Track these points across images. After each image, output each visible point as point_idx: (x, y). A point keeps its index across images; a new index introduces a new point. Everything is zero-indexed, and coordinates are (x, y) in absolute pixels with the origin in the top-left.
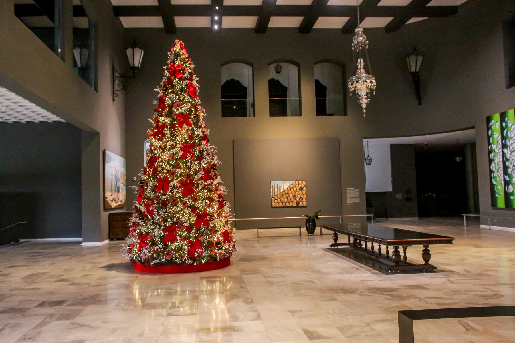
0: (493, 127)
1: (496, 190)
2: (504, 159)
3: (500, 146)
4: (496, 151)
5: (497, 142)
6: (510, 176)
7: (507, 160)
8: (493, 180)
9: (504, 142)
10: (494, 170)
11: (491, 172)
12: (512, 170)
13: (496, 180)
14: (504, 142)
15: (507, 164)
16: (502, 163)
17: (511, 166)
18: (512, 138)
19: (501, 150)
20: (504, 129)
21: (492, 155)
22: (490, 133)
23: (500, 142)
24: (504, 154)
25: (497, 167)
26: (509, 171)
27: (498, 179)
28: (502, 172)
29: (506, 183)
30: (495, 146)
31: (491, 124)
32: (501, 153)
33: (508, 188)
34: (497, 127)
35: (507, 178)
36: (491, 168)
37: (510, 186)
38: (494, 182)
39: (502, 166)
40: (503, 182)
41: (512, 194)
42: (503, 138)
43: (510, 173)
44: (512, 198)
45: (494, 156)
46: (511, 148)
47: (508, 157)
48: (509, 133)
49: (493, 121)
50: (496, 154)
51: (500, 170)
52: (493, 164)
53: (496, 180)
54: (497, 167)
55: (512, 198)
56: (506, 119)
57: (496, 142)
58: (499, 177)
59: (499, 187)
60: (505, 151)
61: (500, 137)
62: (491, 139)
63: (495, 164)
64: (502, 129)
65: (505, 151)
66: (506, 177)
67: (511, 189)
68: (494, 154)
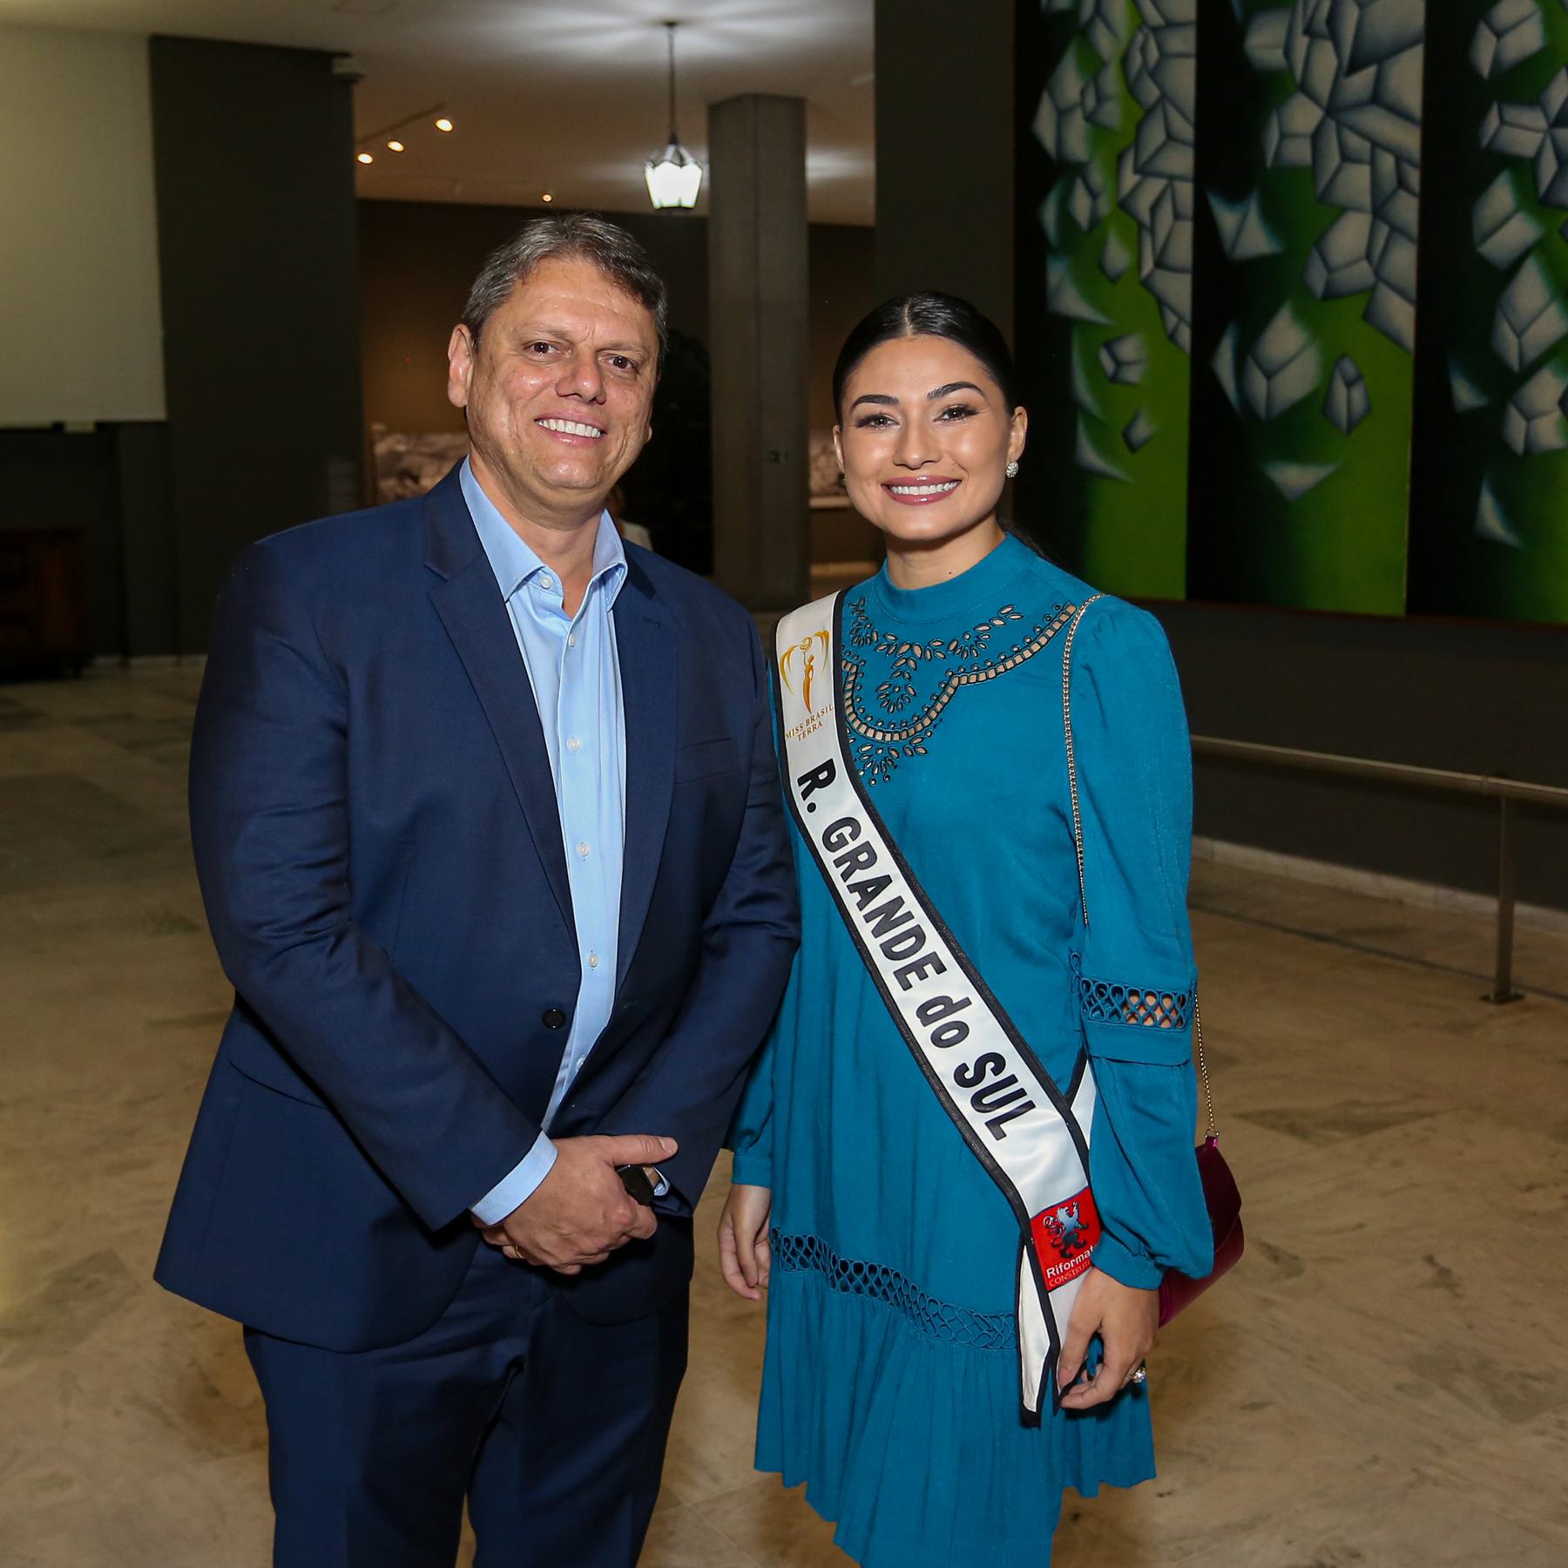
6: (1299, 207)
8: (1057, 272)
12: (1334, 109)
15: (1265, 42)
16: (1184, 41)
17: (1326, 62)
28: (1182, 161)
29: (1232, 297)
33: (1245, 352)
37: (1285, 337)
41: (1300, 429)
43: (1299, 152)
44: (1293, 477)
53: (1095, 275)
55: (1293, 477)
58: (1141, 230)
59: (1129, 349)
63: (1094, 68)
66: (1227, 218)
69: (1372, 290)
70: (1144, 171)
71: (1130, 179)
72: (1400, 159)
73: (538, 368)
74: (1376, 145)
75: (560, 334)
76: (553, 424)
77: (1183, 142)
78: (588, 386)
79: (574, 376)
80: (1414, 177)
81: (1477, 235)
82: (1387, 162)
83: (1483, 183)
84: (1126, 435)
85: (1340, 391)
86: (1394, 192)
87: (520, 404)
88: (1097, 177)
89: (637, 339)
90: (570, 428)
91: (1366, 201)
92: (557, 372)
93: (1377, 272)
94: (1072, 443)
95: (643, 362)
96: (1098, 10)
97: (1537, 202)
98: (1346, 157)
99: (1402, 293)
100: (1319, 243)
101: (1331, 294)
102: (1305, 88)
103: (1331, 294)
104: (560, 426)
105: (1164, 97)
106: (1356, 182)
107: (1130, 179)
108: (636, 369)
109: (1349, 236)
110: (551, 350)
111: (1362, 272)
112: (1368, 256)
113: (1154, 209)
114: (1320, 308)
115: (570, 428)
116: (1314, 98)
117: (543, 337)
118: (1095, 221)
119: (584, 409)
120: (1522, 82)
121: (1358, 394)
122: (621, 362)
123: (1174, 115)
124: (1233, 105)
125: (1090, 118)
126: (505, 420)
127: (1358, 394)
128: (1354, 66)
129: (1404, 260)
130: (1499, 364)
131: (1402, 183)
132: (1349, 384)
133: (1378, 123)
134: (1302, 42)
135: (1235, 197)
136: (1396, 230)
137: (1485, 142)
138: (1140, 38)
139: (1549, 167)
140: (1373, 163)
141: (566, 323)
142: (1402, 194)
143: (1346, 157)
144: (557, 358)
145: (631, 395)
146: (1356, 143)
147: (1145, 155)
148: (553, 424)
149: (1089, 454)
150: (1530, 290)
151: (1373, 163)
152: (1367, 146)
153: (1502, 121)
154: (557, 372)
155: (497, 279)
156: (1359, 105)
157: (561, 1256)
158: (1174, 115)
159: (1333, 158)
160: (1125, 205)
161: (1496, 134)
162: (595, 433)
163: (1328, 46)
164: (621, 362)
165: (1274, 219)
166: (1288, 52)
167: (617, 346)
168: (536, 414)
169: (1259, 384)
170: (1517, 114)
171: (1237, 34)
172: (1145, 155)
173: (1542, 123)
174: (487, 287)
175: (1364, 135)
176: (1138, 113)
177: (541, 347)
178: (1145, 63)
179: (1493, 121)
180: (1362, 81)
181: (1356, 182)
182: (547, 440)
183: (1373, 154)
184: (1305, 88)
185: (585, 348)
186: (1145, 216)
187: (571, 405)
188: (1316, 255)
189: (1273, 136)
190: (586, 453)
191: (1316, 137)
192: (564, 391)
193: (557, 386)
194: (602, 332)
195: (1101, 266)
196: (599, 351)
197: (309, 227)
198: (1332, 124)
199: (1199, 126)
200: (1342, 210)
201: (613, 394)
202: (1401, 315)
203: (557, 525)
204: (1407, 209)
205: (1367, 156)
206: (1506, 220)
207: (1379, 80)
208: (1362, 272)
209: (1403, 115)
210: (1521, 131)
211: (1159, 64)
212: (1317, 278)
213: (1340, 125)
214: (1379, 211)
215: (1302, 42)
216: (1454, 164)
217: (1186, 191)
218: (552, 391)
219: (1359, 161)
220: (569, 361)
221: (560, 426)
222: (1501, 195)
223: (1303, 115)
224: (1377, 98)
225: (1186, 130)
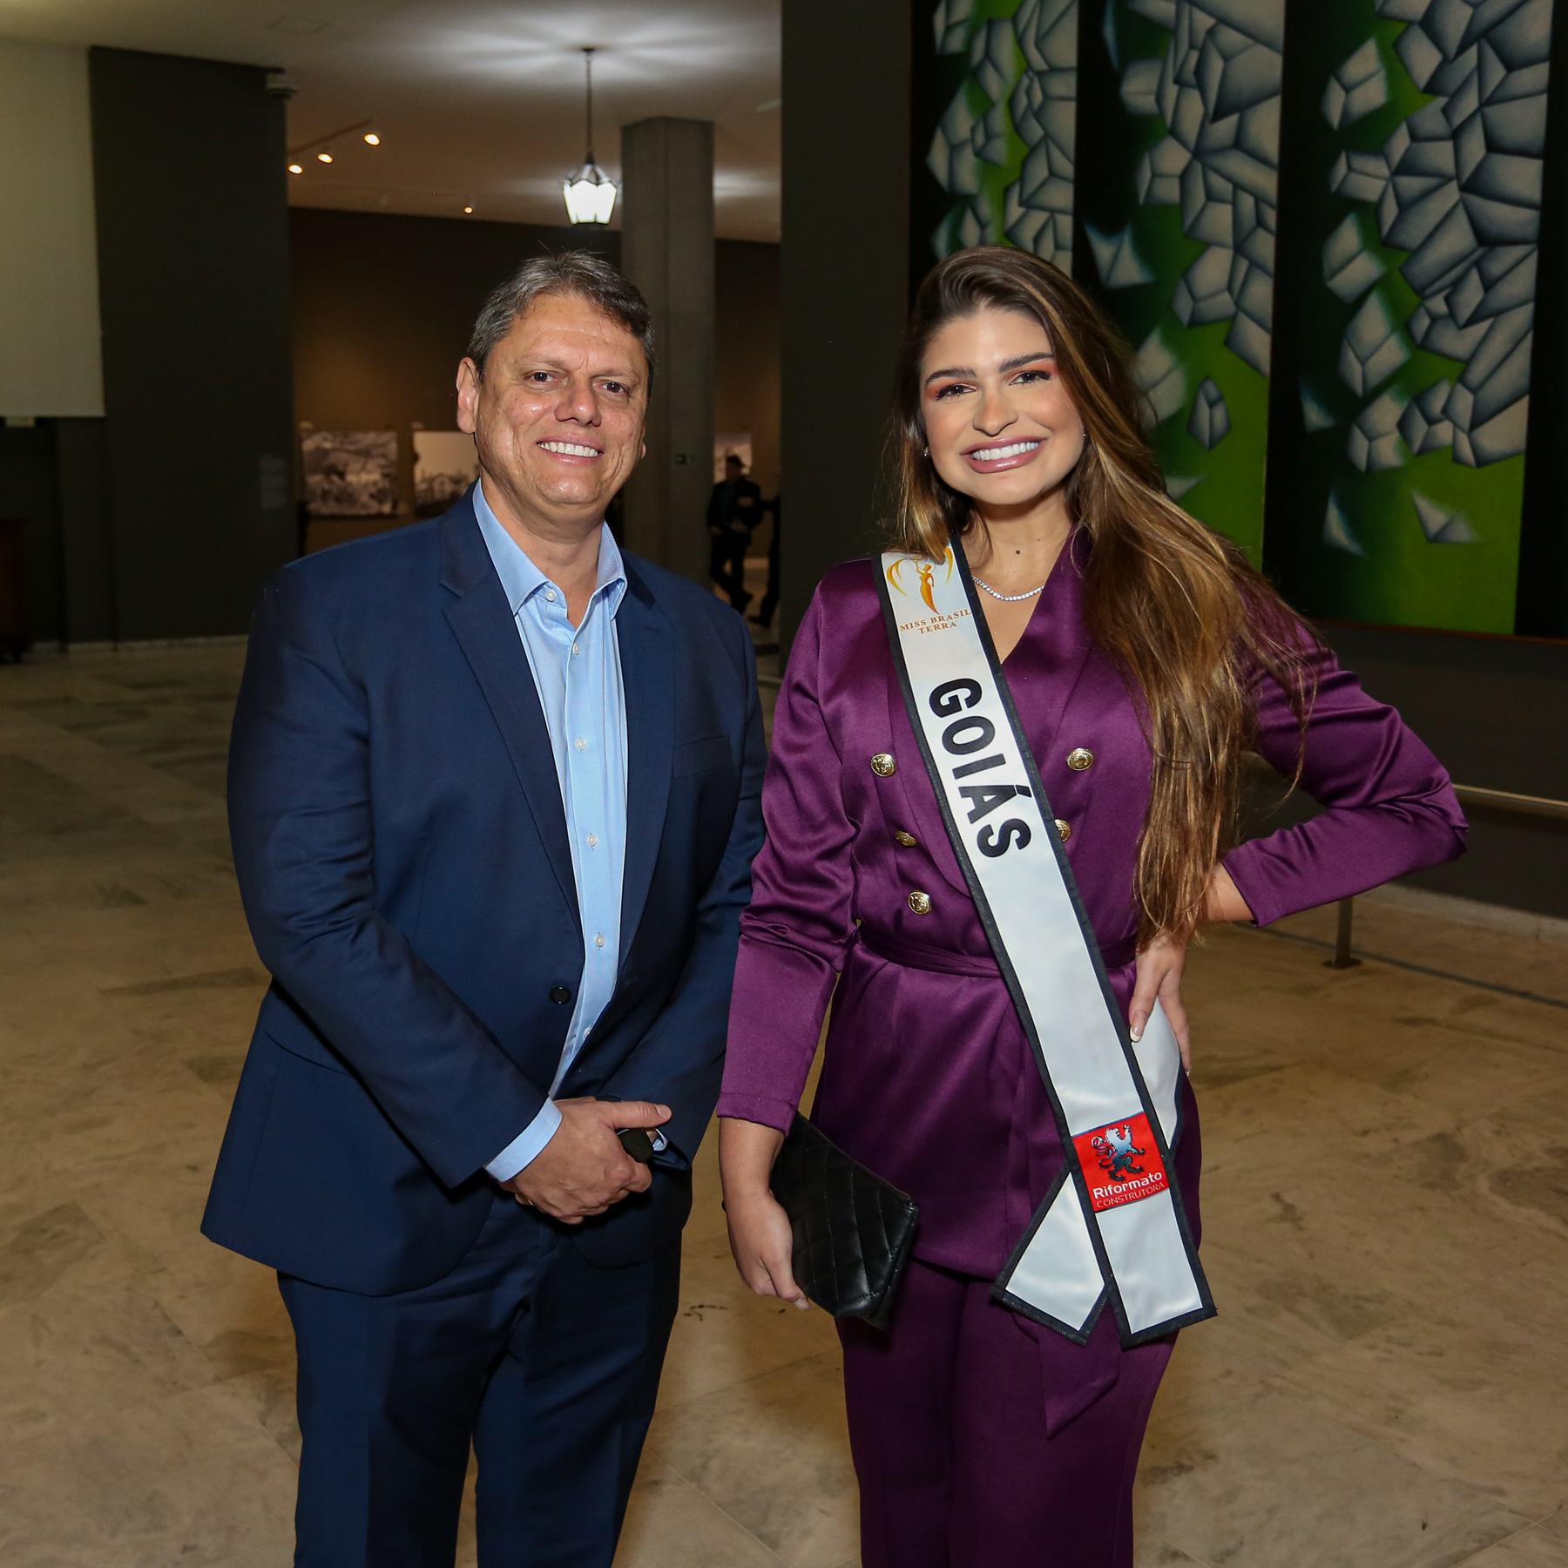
2: (1109, 32)
6: (1168, 241)
7: (1147, 38)
10: (967, 177)
11: (934, 203)
12: (1200, 153)
16: (1065, 86)
17: (1193, 109)
28: (1062, 196)
35: (1122, 264)
36: (938, 159)
39: (1065, 119)
43: (1169, 191)
45: (984, 21)
51: (1039, 171)
52: (961, 118)
54: (1001, 150)
66: (1103, 250)
69: (1232, 319)
70: (1028, 204)
71: (1015, 211)
72: (1259, 200)
73: (538, 396)
74: (1238, 186)
75: (556, 364)
76: (553, 447)
77: (1064, 179)
78: (584, 411)
79: (571, 401)
80: (1271, 217)
81: (1327, 271)
82: (1247, 202)
83: (1330, 226)
86: (1254, 229)
87: (523, 429)
88: (986, 208)
89: (627, 365)
90: (569, 449)
91: (1229, 239)
92: (555, 399)
93: (1237, 303)
95: (634, 386)
96: (988, 55)
97: (1381, 243)
98: (1211, 197)
99: (1260, 323)
100: (1186, 274)
101: (1196, 322)
102: (1174, 132)
103: (1196, 322)
104: (561, 448)
105: (1047, 136)
106: (1219, 220)
107: (1015, 211)
108: (628, 393)
109: (1213, 270)
110: (549, 379)
111: (1225, 302)
112: (1230, 288)
113: (1037, 240)
115: (569, 449)
116: (1183, 143)
117: (542, 367)
119: (581, 432)
120: (1366, 134)
122: (614, 387)
123: (1057, 155)
124: (1110, 144)
125: (978, 154)
126: (509, 444)
128: (1219, 114)
129: (1261, 292)
130: (1344, 388)
131: (1260, 222)
133: (1239, 166)
134: (1172, 90)
135: (1111, 229)
136: (1255, 265)
137: (1334, 187)
138: (1026, 82)
139: (1390, 212)
140: (1235, 204)
141: (562, 353)
142: (1261, 232)
143: (1211, 197)
144: (555, 386)
145: (624, 418)
146: (1219, 184)
147: (1029, 189)
148: (553, 447)
150: (1373, 323)
151: (1235, 204)
152: (1230, 186)
153: (1350, 168)
154: (555, 399)
155: (498, 314)
156: (1221, 150)
157: (564, 1208)
158: (1057, 155)
161: (1344, 180)
162: (592, 453)
163: (1193, 98)
164: (614, 387)
165: (1146, 251)
166: (1159, 98)
167: (610, 373)
168: (536, 438)
170: (1361, 162)
172: (1029, 189)
173: (1385, 172)
174: (489, 322)
175: (1228, 178)
176: (1025, 151)
177: (540, 377)
178: (1030, 104)
179: (1341, 168)
181: (1219, 220)
182: (548, 460)
183: (1234, 194)
185: (581, 376)
186: (1030, 246)
187: (570, 429)
188: (1182, 283)
189: (1146, 174)
190: (583, 471)
191: (1184, 177)
192: (563, 416)
193: (556, 412)
194: (597, 360)
196: (593, 378)
197: (287, 250)
198: (1198, 167)
199: (1079, 164)
200: (1206, 245)
201: (607, 416)
202: (1258, 342)
203: (563, 538)
204: (1265, 246)
205: (1229, 197)
206: (1352, 259)
207: (1240, 130)
208: (1225, 302)
209: (1263, 160)
210: (1366, 178)
211: (1042, 106)
212: (1184, 307)
213: (1204, 166)
214: (1240, 248)
216: (1306, 207)
217: (1066, 224)
218: (552, 416)
219: (1222, 201)
220: (567, 388)
221: (561, 448)
222: (1348, 236)
223: (1172, 157)
224: (1239, 143)
225: (1067, 167)
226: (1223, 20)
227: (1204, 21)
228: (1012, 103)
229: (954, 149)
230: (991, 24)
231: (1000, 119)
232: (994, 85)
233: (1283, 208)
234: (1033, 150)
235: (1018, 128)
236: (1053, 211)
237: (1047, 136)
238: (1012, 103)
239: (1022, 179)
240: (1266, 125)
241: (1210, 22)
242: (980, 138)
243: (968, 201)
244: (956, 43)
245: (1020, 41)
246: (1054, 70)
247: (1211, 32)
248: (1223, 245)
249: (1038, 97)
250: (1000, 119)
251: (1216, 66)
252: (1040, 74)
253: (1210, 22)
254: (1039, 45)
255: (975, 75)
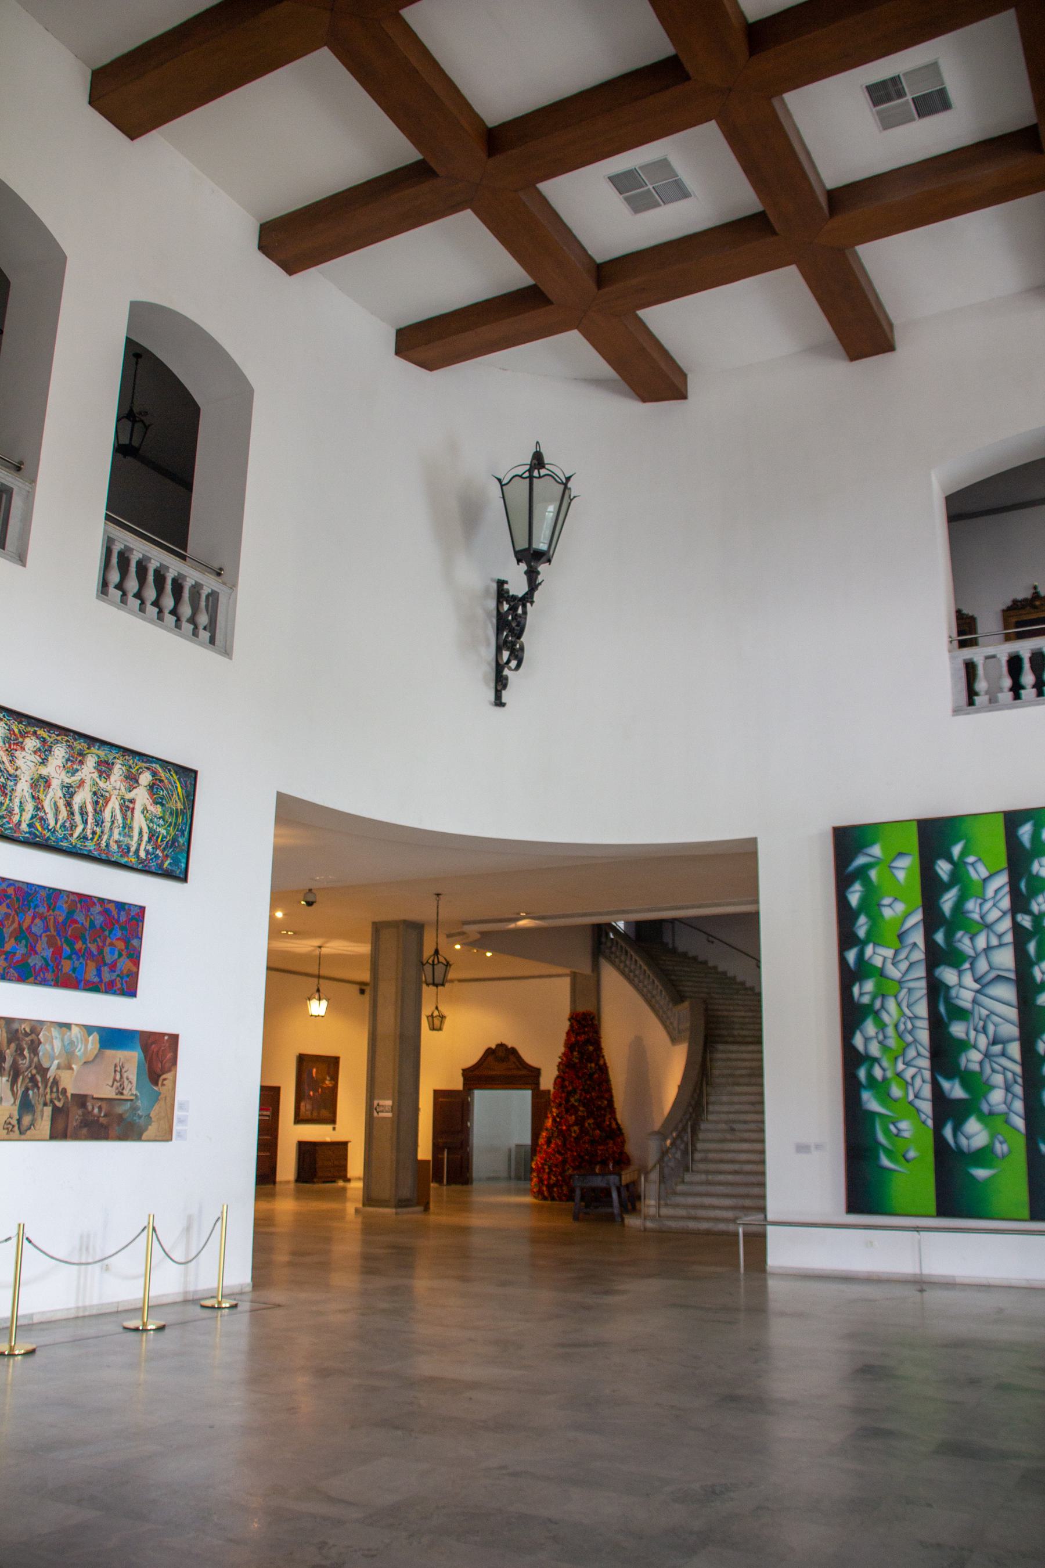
0: (873, 874)
1: (881, 1137)
2: (942, 1009)
3: (919, 955)
4: (894, 973)
5: (901, 937)
7: (960, 1014)
8: (866, 1095)
9: (939, 937)
10: (874, 1050)
12: (987, 1055)
13: (885, 1097)
14: (939, 937)
16: (924, 1024)
17: (982, 1041)
18: (988, 927)
19: (921, 972)
20: (946, 887)
21: (864, 991)
22: (854, 898)
23: (918, 937)
24: (936, 990)
25: (892, 1042)
26: (972, 1059)
27: (896, 1091)
28: (925, 1063)
29: (946, 1110)
30: (889, 953)
31: (861, 860)
32: (923, 984)
34: (901, 875)
35: (955, 1090)
36: (858, 1041)
37: (973, 1125)
38: (871, 1102)
40: (926, 1107)
42: (933, 918)
46: (982, 966)
47: (967, 1005)
48: (971, 905)
49: (876, 850)
50: (893, 987)
51: (911, 1053)
52: (870, 1027)
53: (885, 1097)
54: (892, 1042)
56: (956, 850)
57: (891, 937)
59: (903, 1125)
60: (948, 975)
61: (918, 917)
62: (862, 920)
63: (882, 1026)
64: (931, 887)
65: (948, 975)
66: (946, 1085)
67: (975, 1133)
68: (878, 985)
70: (907, 1064)
71: (901, 1066)
72: (1014, 1074)
74: (1005, 1068)
80: (1020, 1080)
82: (1009, 1075)
84: (904, 1156)
85: (998, 1146)
94: (878, 1158)
100: (985, 1097)
101: (991, 1114)
109: (997, 1097)
112: (1005, 1103)
113: (913, 1078)
114: (987, 1118)
116: (979, 1051)
118: (885, 1079)
121: (1005, 1147)
123: (919, 1047)
127: (1005, 1147)
128: (995, 1042)
129: (1018, 1105)
131: (1016, 1082)
132: (1001, 1143)
134: (972, 1034)
135: (949, 1077)
136: (1015, 1096)
140: (1004, 1074)
143: (993, 1071)
149: (885, 1162)
159: (988, 1070)
160: (899, 1075)
165: (965, 1085)
169: (963, 1142)
171: (946, 1026)
180: (997, 1048)
181: (998, 1079)
184: (975, 1047)
186: (909, 1080)
195: (889, 1095)
200: (993, 1087)
204: (1018, 1090)
212: (985, 1108)
214: (1008, 1089)
215: (972, 1034)
217: (927, 1074)
224: (1003, 1054)
226: (992, 1013)
227: (984, 1012)
228: (896, 1026)
229: (867, 1040)
230: (883, 996)
231: (890, 1031)
232: (885, 1017)
233: (1024, 1077)
234: (908, 1045)
235: (900, 1036)
236: (920, 1068)
237: (915, 1041)
238: (896, 1026)
239: (903, 1055)
240: (1015, 1049)
241: (987, 1012)
242: (881, 1037)
243: (876, 1060)
244: (866, 1000)
245: (899, 1005)
246: (916, 1017)
247: (988, 1016)
248: (999, 1088)
249: (909, 1026)
250: (890, 1031)
251: (991, 1029)
252: (910, 1018)
253: (987, 1012)
254: (908, 1006)
255: (877, 1013)
